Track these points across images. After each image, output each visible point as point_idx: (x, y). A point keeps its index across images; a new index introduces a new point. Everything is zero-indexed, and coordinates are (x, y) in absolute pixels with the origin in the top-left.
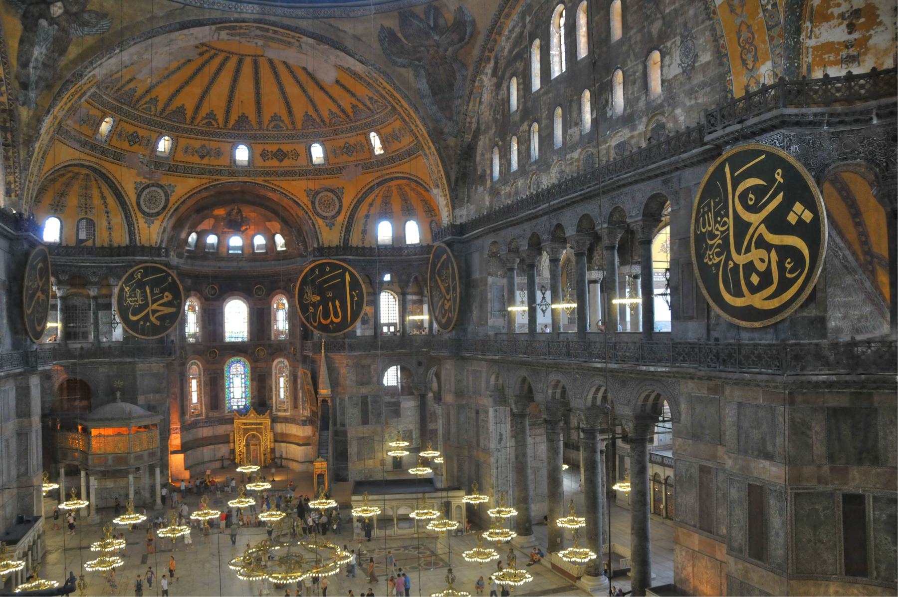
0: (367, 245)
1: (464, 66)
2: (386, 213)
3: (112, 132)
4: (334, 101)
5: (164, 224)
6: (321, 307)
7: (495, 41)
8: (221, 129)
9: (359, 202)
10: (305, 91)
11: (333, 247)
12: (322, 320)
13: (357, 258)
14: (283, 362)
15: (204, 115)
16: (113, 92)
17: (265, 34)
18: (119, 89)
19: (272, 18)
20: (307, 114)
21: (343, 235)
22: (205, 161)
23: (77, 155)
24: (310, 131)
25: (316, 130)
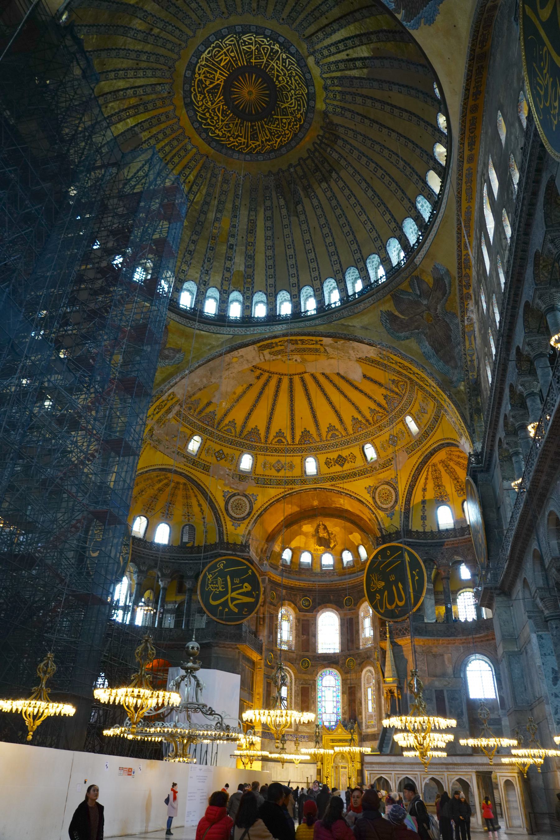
0: (428, 529)
1: (454, 315)
3: (201, 448)
4: (370, 398)
5: (249, 528)
6: (386, 593)
7: (468, 276)
9: (412, 487)
10: (346, 396)
12: (388, 606)
13: (417, 541)
14: (370, 671)
16: (196, 413)
17: (295, 346)
18: (200, 412)
19: (296, 330)
20: (354, 419)
23: (172, 462)
24: (360, 433)
25: (364, 431)
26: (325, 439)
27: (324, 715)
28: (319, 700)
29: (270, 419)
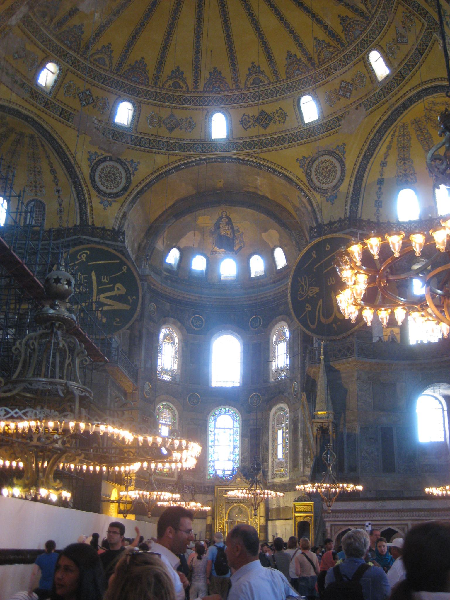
2: (406, 176)
4: (319, 21)
5: (124, 209)
6: (320, 302)
8: (191, 92)
10: (281, 18)
11: (335, 222)
12: (322, 320)
14: (282, 409)
15: (170, 74)
18: (60, 24)
20: (290, 55)
21: (348, 208)
22: (174, 134)
23: (14, 97)
25: (304, 75)
26: (243, 86)
27: (216, 463)
28: (210, 444)
29: (164, 49)
